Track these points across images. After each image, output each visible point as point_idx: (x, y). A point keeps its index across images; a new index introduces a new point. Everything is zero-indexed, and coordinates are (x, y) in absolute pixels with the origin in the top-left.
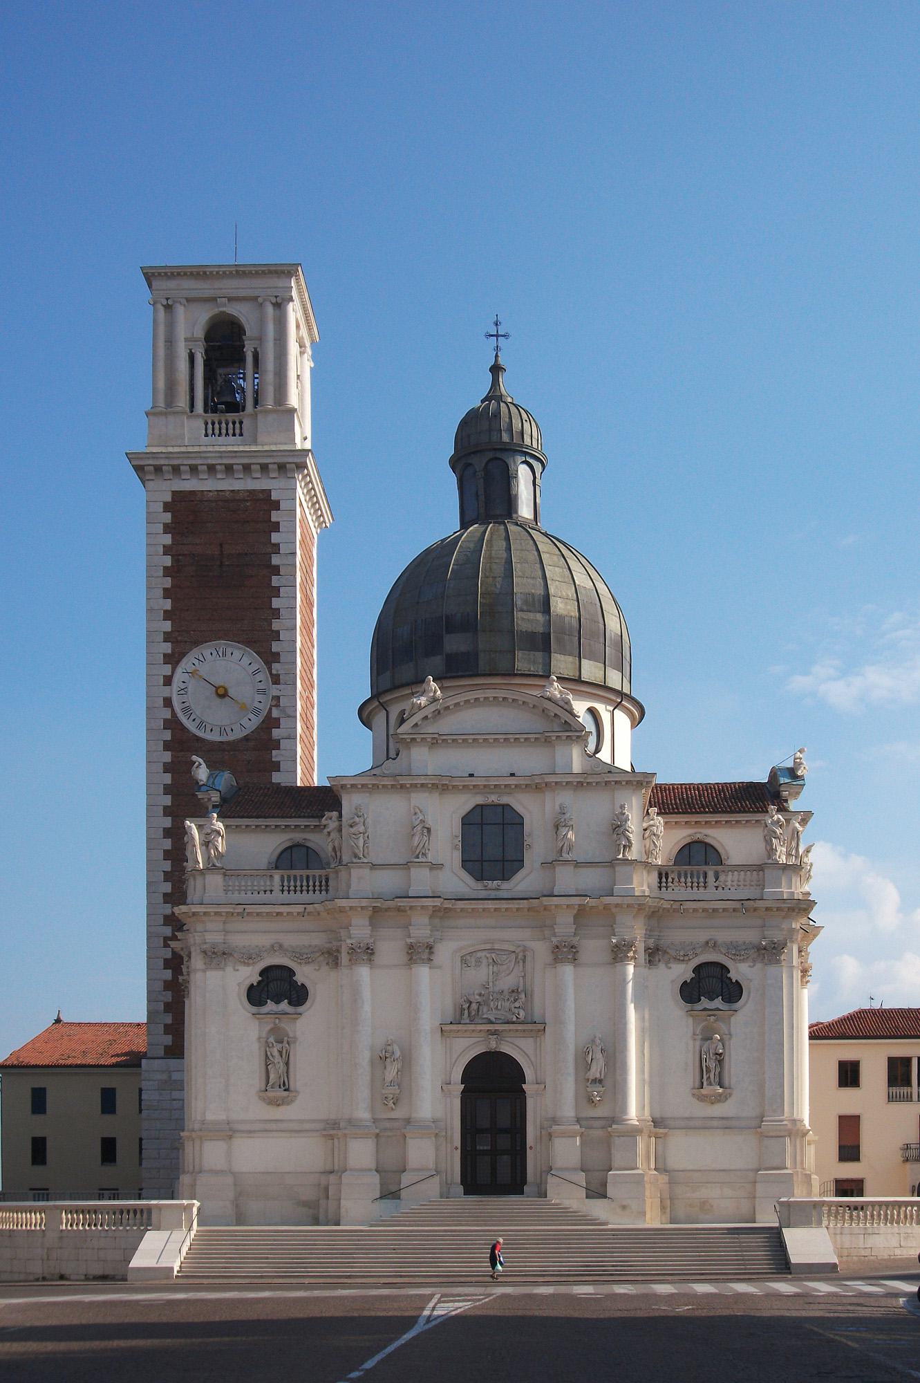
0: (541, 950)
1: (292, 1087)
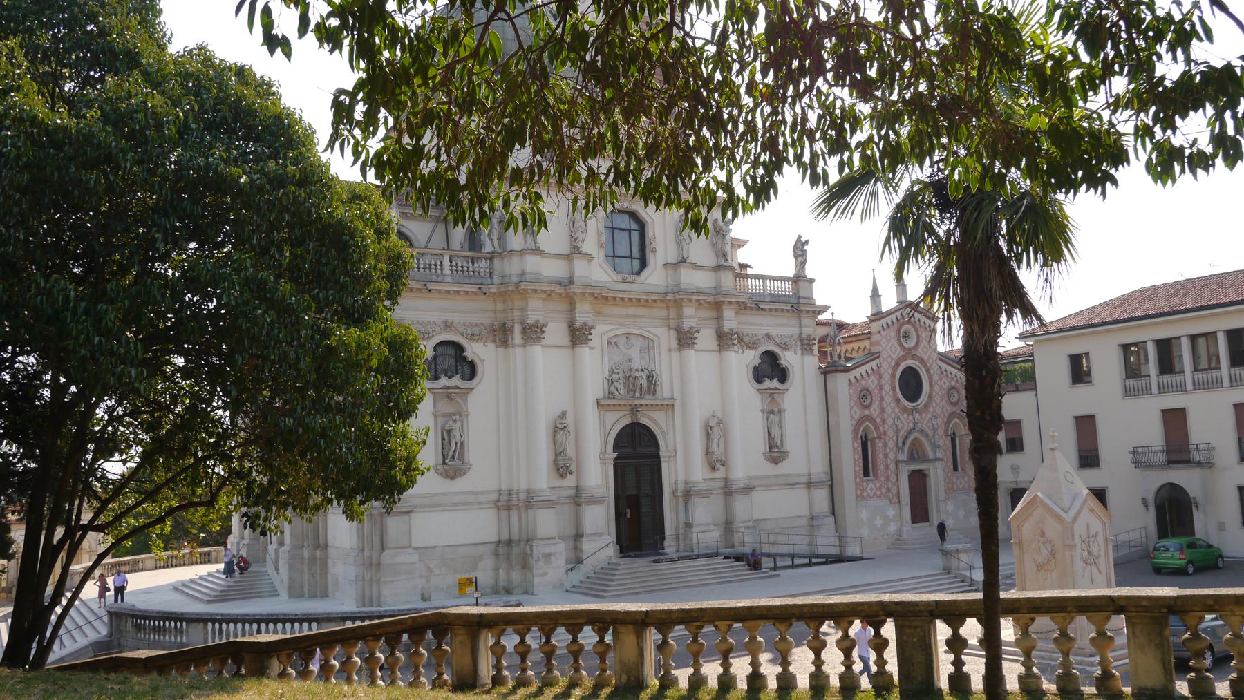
0: (665, 338)
1: (466, 461)
